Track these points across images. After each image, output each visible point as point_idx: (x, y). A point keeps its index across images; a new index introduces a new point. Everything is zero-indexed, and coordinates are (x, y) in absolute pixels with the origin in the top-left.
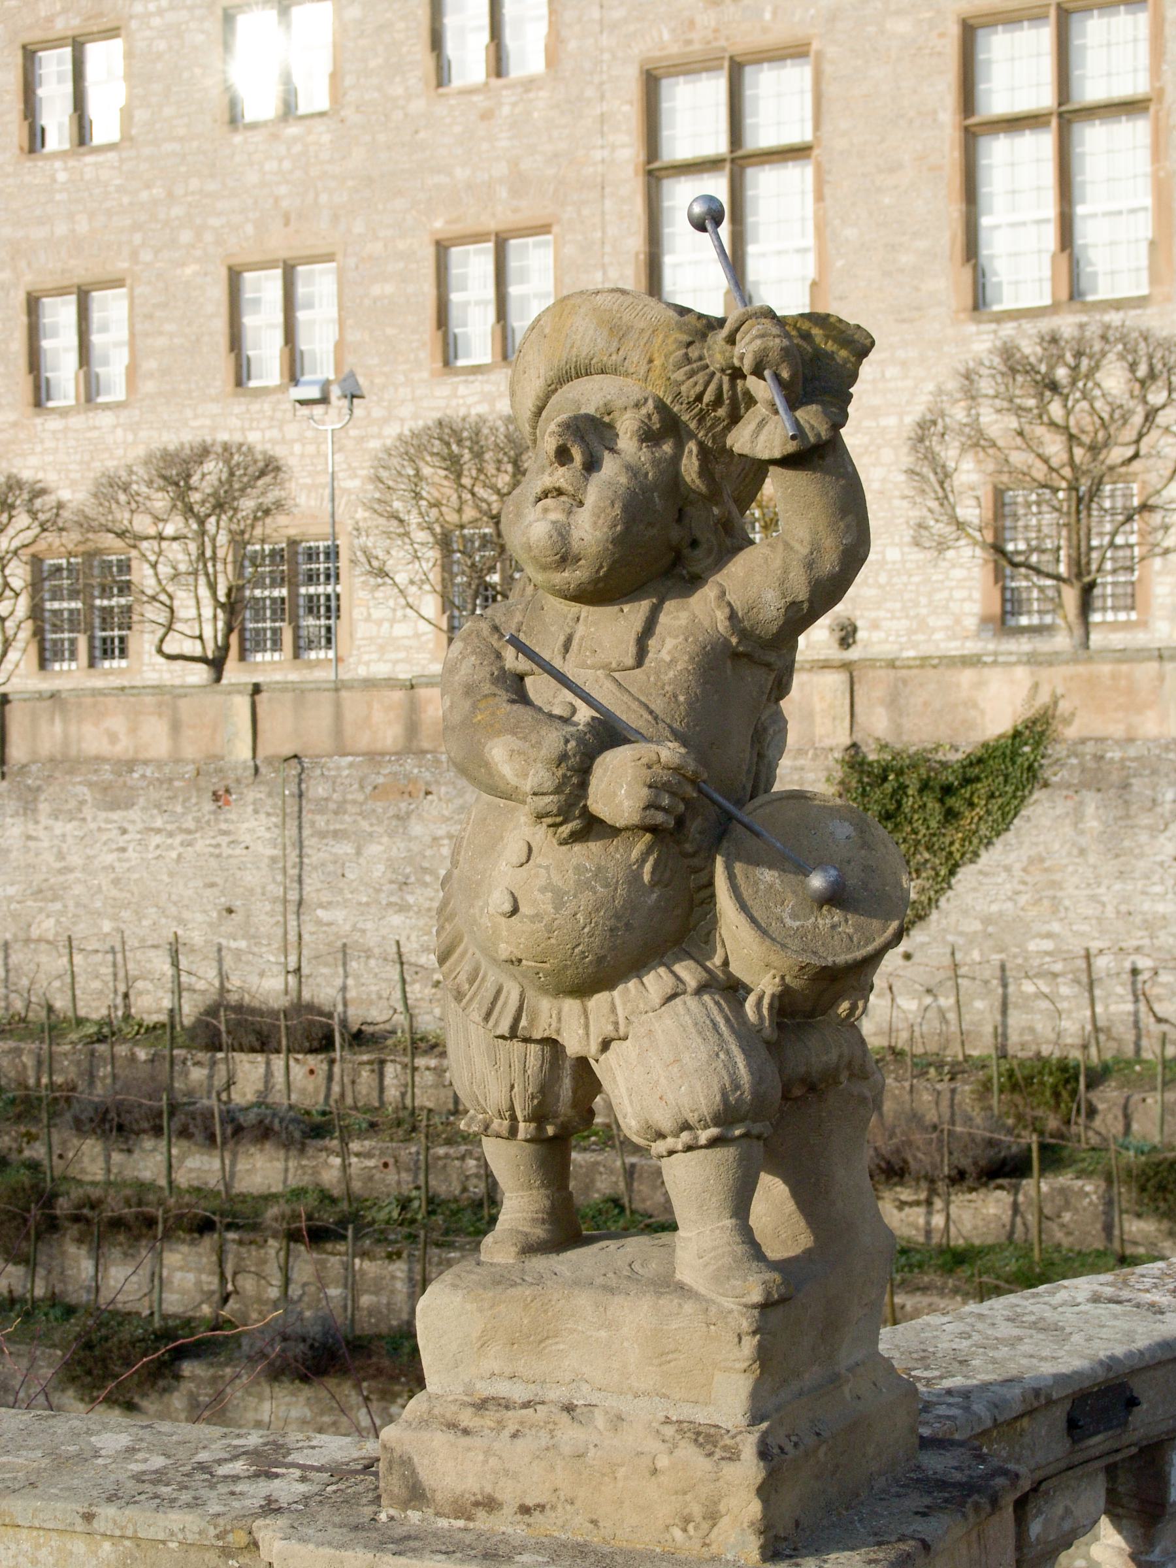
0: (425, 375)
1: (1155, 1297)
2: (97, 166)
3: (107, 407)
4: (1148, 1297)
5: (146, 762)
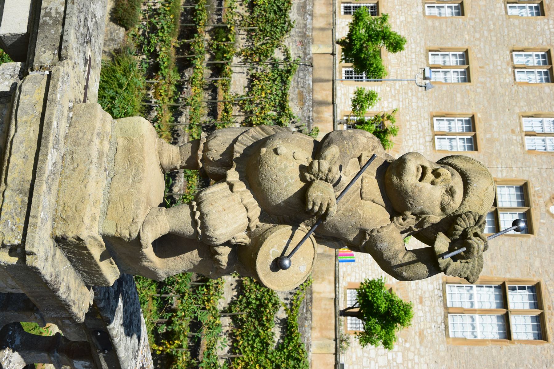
0: (431, 110)
1: (140, 357)
2: (500, 8)
3: (424, 9)
4: (140, 354)
5: (312, 19)
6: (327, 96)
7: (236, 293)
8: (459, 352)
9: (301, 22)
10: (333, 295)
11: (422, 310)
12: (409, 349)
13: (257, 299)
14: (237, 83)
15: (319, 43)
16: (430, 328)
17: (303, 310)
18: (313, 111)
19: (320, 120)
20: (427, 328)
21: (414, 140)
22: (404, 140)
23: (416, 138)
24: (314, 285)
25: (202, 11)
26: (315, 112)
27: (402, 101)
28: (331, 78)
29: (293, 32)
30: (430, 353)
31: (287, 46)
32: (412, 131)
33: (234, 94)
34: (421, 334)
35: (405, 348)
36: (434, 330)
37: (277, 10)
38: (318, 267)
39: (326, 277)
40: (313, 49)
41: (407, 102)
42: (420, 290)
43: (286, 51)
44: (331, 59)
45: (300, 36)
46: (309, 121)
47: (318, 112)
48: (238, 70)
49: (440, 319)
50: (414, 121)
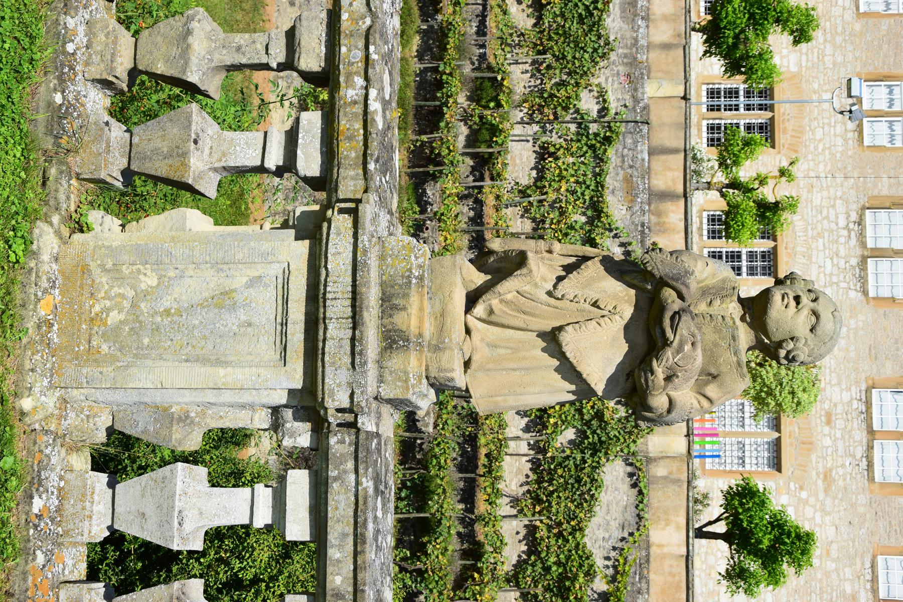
5: (647, 26)
6: (674, 180)
7: (525, 548)
8: (889, 506)
9: (628, 35)
10: (683, 551)
11: (830, 435)
12: (806, 502)
13: (558, 563)
14: (518, 161)
15: (660, 75)
16: (843, 466)
17: (634, 578)
18: (649, 211)
19: (663, 229)
20: (837, 467)
21: (826, 128)
22: (808, 128)
23: (829, 124)
24: (651, 533)
25: (451, 74)
26: (653, 214)
27: (807, 54)
28: (682, 146)
29: (613, 56)
30: (842, 508)
31: (603, 85)
32: (823, 110)
33: (513, 183)
34: (827, 476)
35: (800, 499)
36: (849, 469)
37: (583, 13)
38: (659, 501)
39: (672, 518)
40: (651, 90)
41: (816, 55)
42: (827, 402)
43: (602, 96)
44: (681, 108)
45: (626, 64)
46: (643, 232)
47: (659, 214)
48: (518, 130)
49: (860, 451)
50: (826, 92)
